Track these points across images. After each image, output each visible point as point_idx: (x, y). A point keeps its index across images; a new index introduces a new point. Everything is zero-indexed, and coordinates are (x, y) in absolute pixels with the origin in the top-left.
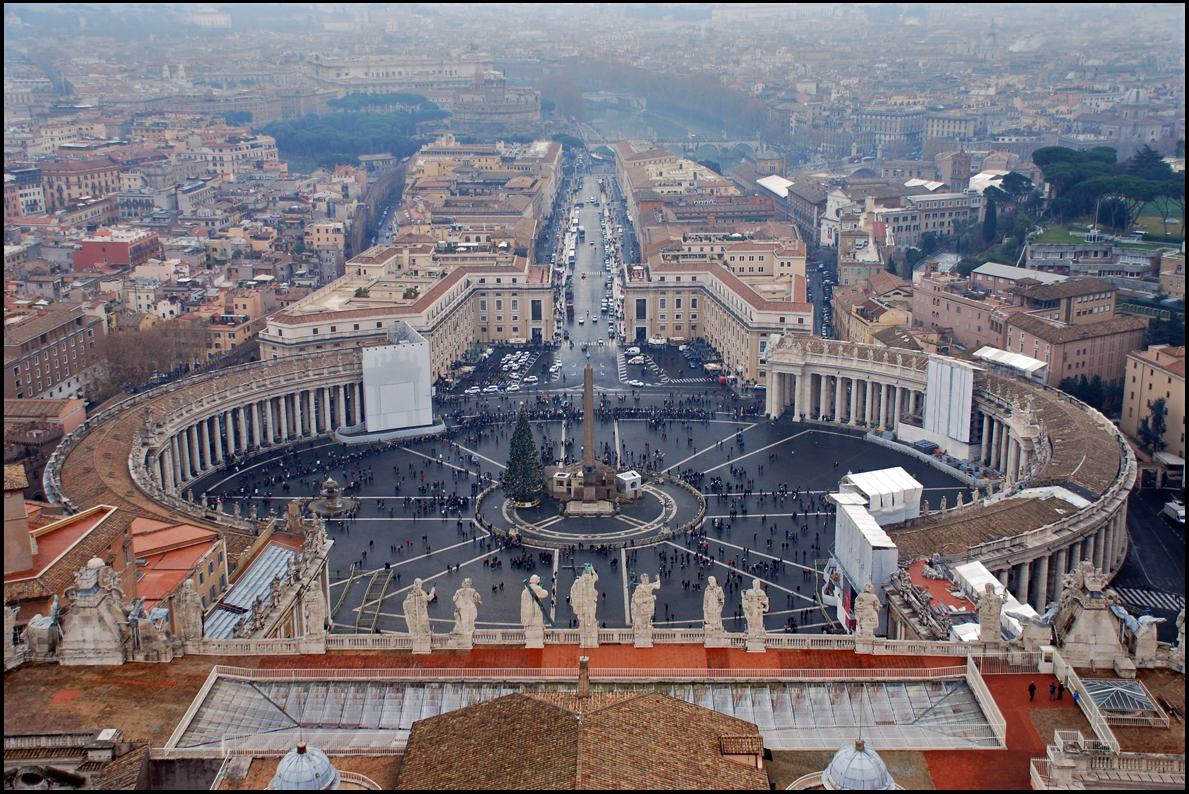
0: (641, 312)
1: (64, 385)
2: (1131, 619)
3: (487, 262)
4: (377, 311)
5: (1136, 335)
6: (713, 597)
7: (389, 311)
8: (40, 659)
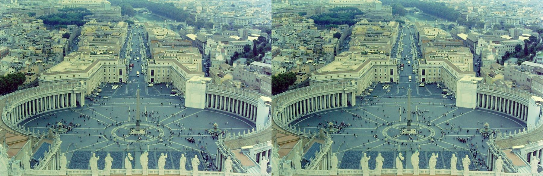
3: (106, 58)
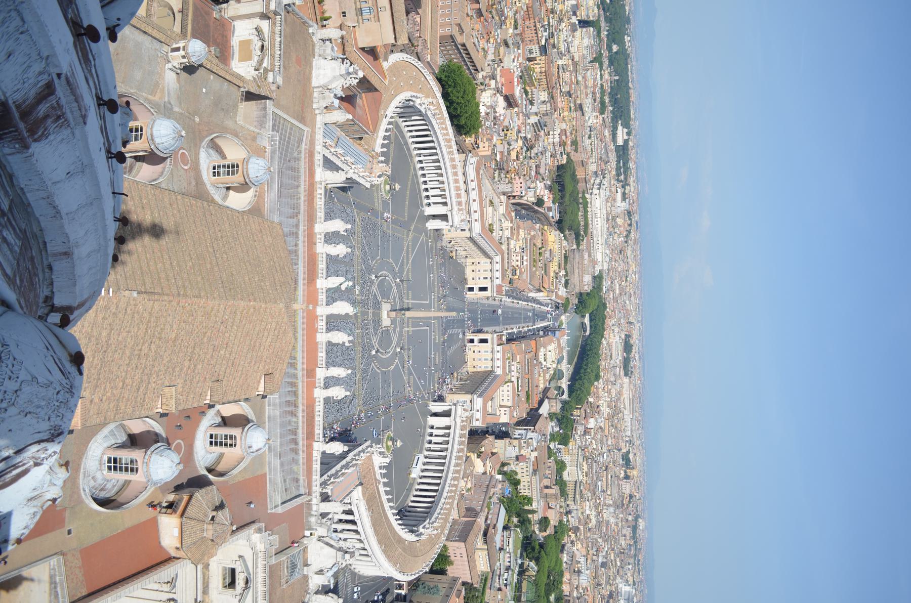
2: (331, 573)
4: (482, 211)
5: (469, 581)
6: (340, 372)
7: (482, 216)
8: (316, 50)
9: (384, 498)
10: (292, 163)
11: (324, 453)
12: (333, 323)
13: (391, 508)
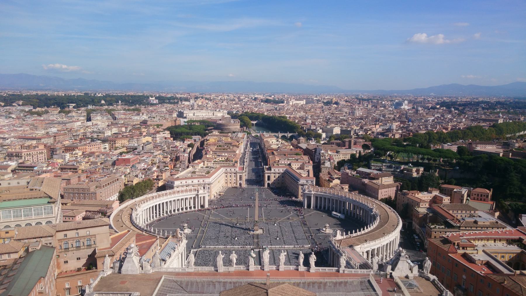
0: (269, 179)
1: (113, 197)
2: (412, 264)
7: (202, 178)
9: (359, 233)
10: (184, 286)
11: (345, 267)
12: (274, 260)
13: (364, 230)
